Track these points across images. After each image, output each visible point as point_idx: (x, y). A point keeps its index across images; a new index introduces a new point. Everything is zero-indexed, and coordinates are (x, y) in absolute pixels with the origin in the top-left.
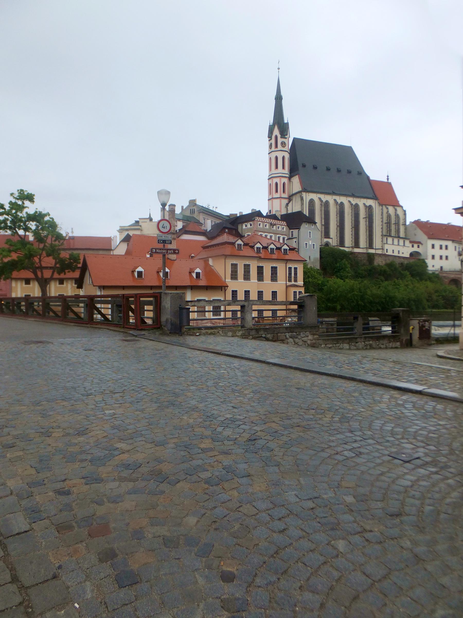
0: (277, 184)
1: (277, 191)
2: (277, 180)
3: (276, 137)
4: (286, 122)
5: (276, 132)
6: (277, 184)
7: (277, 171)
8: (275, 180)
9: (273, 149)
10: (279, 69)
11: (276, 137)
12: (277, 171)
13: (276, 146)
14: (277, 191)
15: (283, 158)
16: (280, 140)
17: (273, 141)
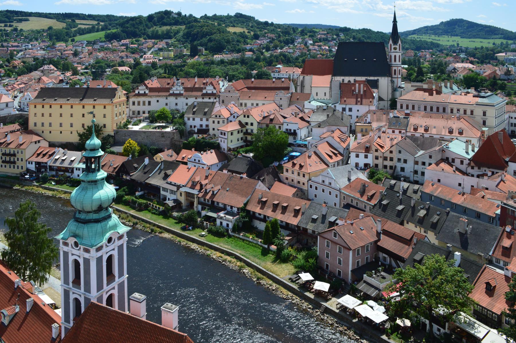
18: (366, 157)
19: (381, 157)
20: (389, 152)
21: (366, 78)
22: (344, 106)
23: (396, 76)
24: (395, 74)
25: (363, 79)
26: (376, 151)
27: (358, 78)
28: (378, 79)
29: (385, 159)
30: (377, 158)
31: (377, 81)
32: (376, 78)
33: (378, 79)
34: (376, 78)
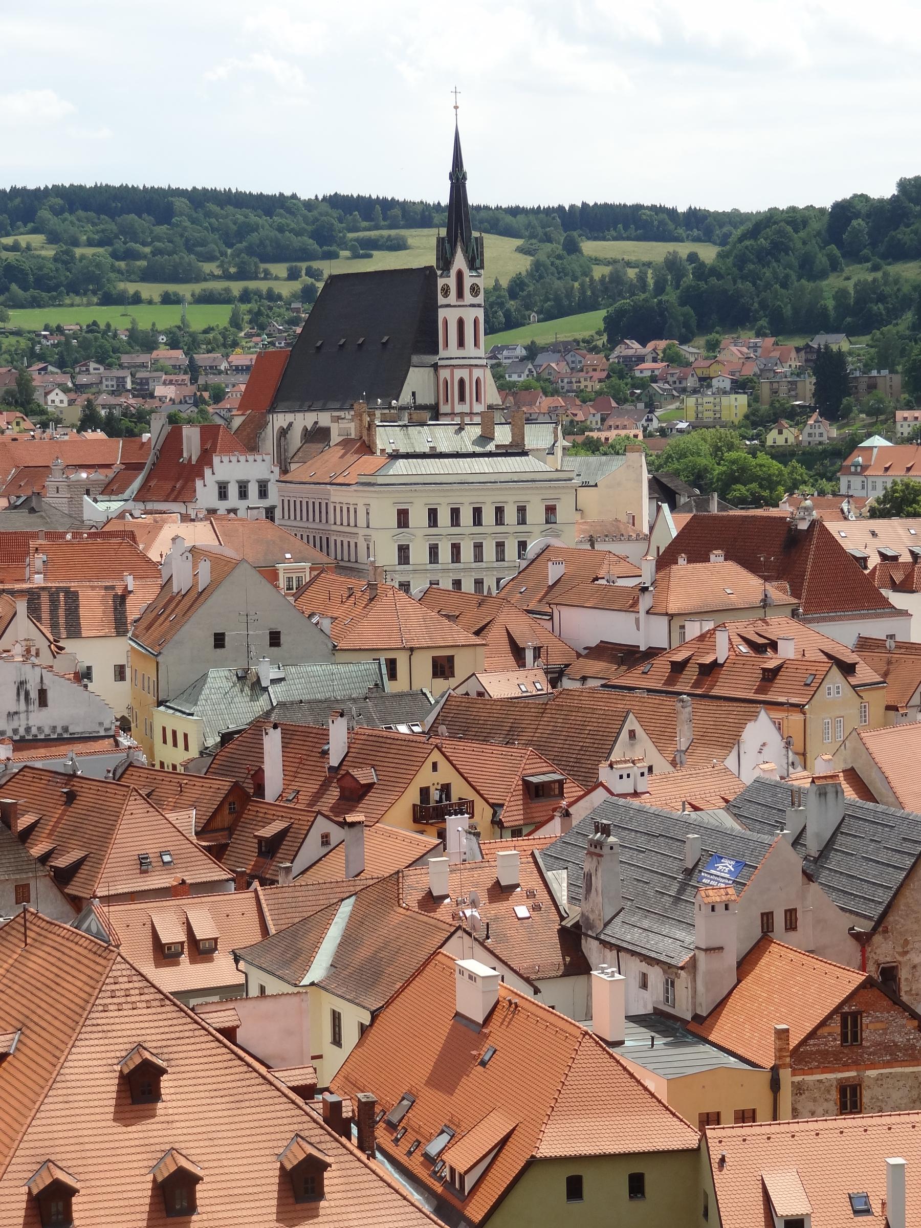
0: (462, 382)
1: (462, 398)
2: (463, 373)
3: (460, 275)
5: (460, 262)
6: (462, 382)
7: (461, 353)
8: (459, 374)
9: (452, 298)
10: (456, 107)
11: (460, 275)
12: (461, 353)
13: (460, 295)
15: (476, 321)
16: (468, 283)
17: (452, 282)
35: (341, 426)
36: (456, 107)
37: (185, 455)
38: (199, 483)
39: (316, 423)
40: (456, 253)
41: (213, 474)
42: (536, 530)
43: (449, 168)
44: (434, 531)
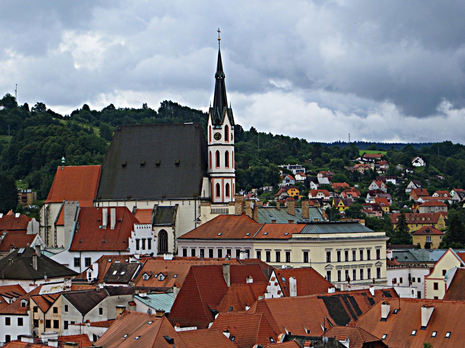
0: (227, 185)
1: (227, 195)
3: (226, 127)
4: (229, 107)
6: (227, 185)
8: (226, 181)
9: (222, 140)
11: (226, 127)
14: (227, 195)
17: (222, 132)
18: (20, 322)
19: (41, 321)
20: (52, 309)
21: (156, 203)
22: (77, 255)
23: (220, 200)
24: (218, 195)
25: (151, 205)
26: (35, 310)
27: (142, 205)
28: (177, 205)
29: (48, 324)
30: (36, 323)
31: (174, 209)
32: (173, 204)
33: (177, 205)
34: (173, 204)
35: (212, 208)
36: (219, 40)
37: (105, 223)
38: (130, 240)
39: (135, 207)
40: (224, 116)
41: (135, 235)
42: (374, 262)
43: (215, 71)
44: (339, 264)
